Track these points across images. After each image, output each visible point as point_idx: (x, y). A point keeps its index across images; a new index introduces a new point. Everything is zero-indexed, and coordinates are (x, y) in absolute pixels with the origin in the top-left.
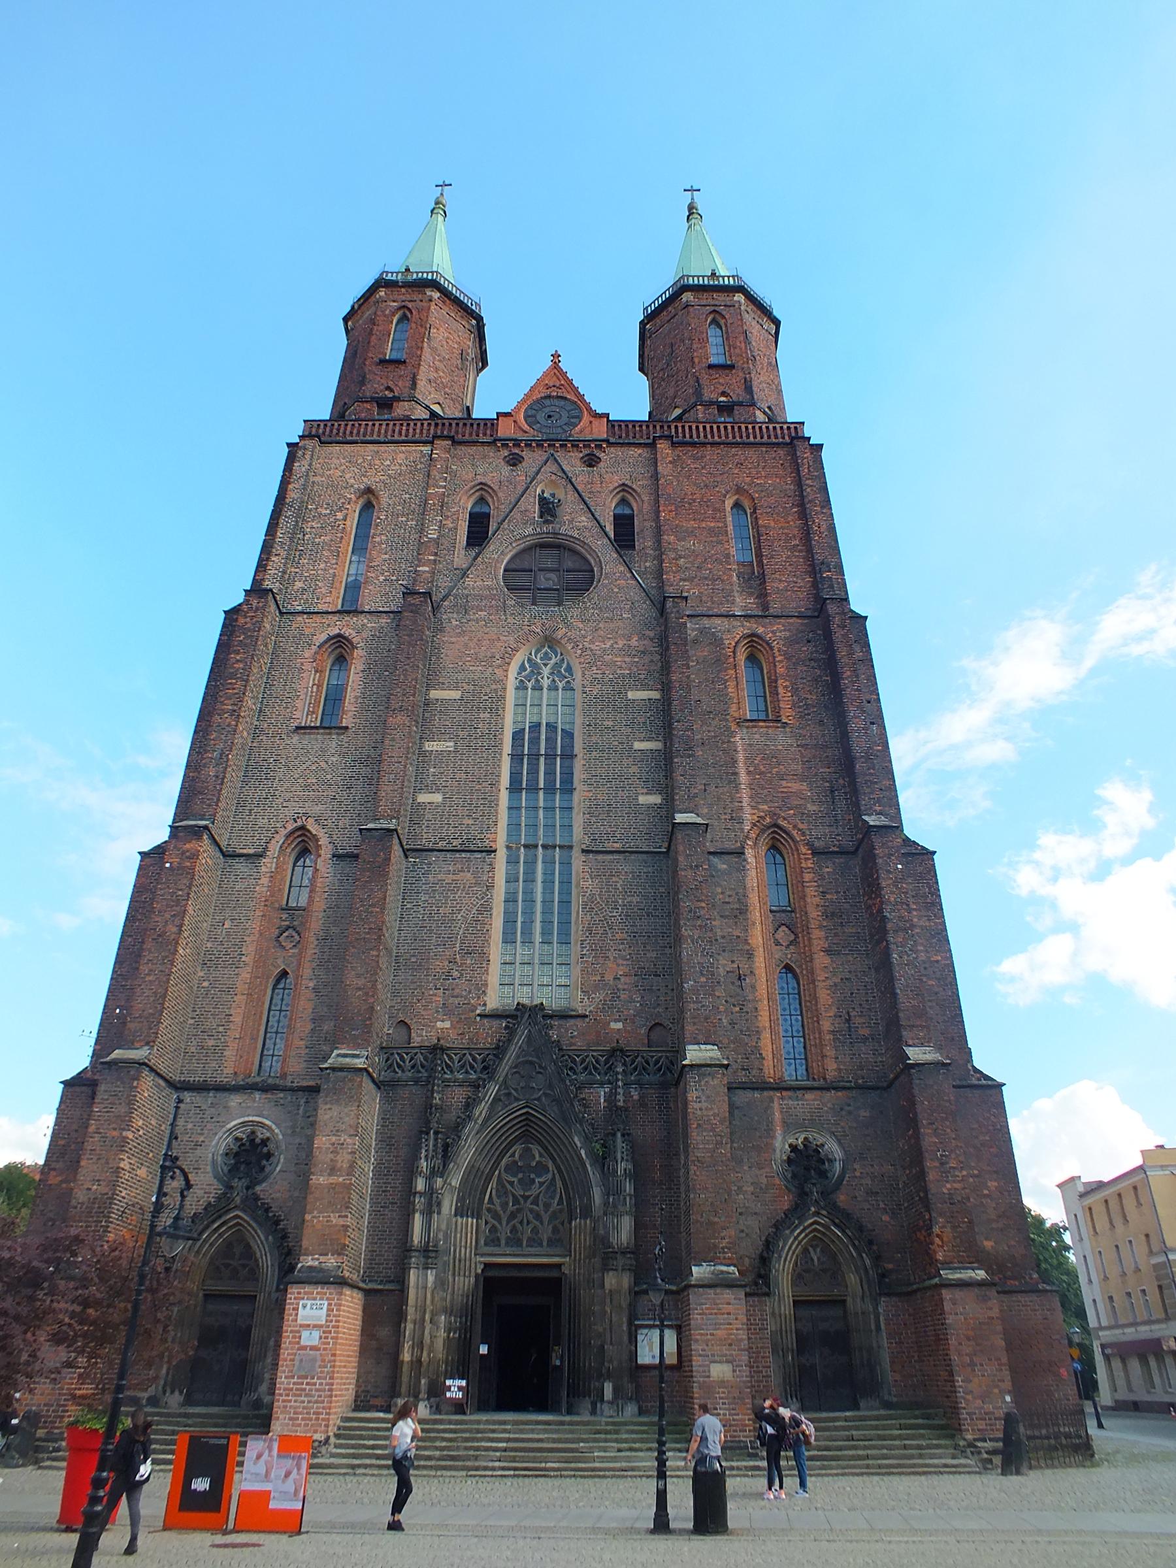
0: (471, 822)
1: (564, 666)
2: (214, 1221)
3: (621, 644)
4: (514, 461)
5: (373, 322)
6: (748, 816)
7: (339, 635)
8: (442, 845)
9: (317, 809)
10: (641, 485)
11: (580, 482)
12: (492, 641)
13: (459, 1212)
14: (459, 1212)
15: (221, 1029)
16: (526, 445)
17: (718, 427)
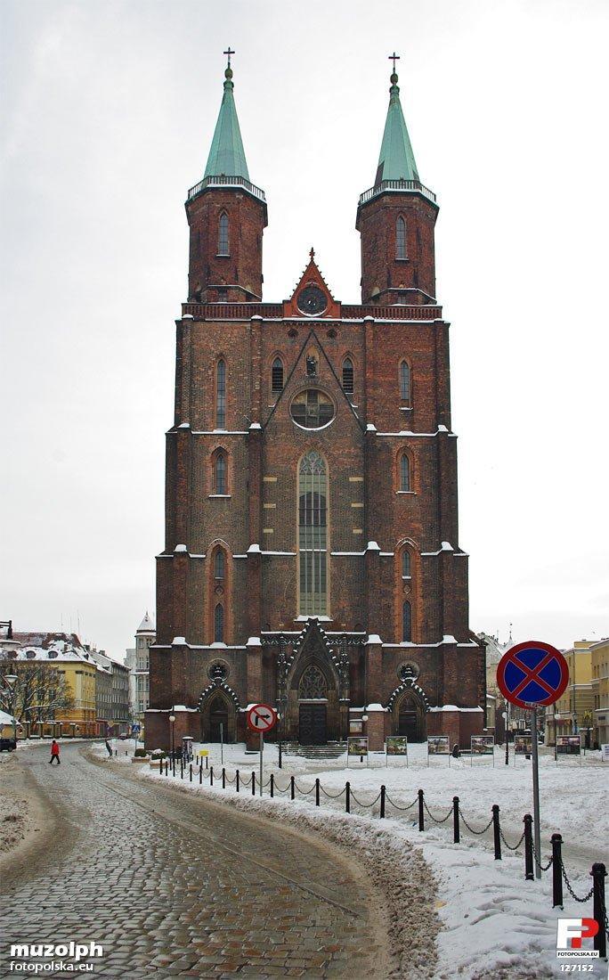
10: (357, 351)
13: (292, 688)
14: (292, 688)
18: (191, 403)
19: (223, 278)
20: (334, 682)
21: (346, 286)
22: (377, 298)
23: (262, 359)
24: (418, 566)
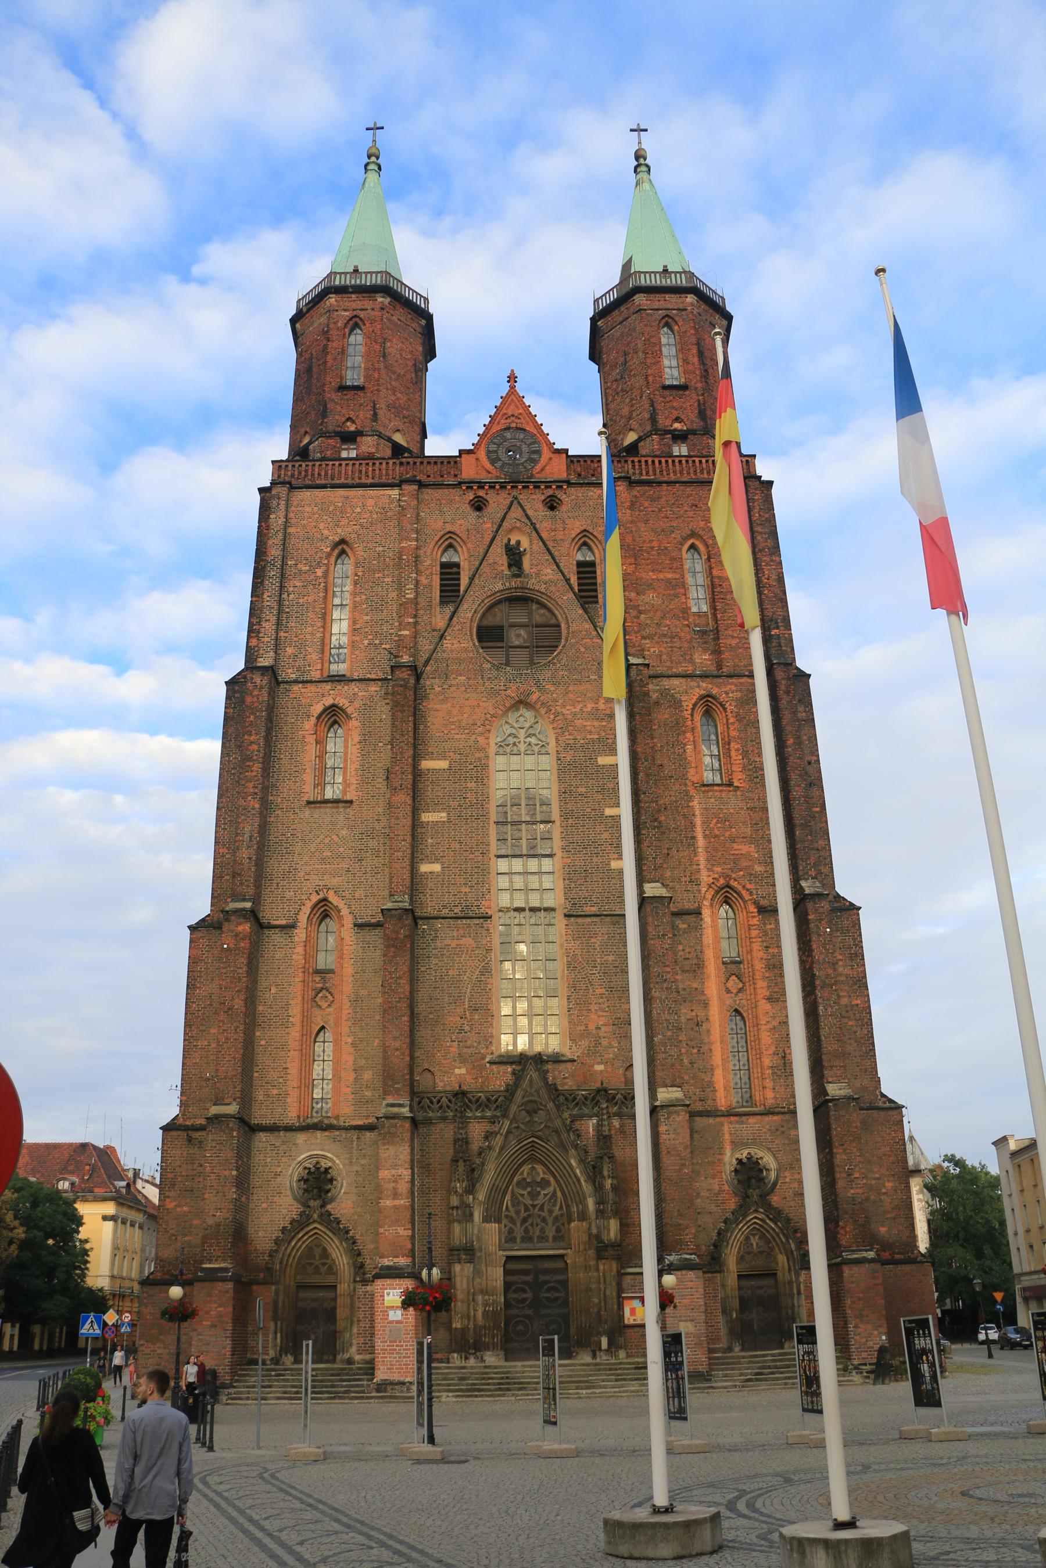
0: (468, 890)
2: (298, 1233)
3: (590, 706)
4: (479, 505)
5: (325, 333)
6: (705, 877)
7: (333, 705)
8: (445, 912)
9: (335, 881)
11: (543, 527)
12: (473, 707)
13: (486, 1219)
14: (486, 1219)
15: (281, 1080)
16: (490, 487)
17: (673, 461)
19: (349, 419)
20: (583, 1201)
22: (633, 449)
23: (417, 548)
24: (754, 933)
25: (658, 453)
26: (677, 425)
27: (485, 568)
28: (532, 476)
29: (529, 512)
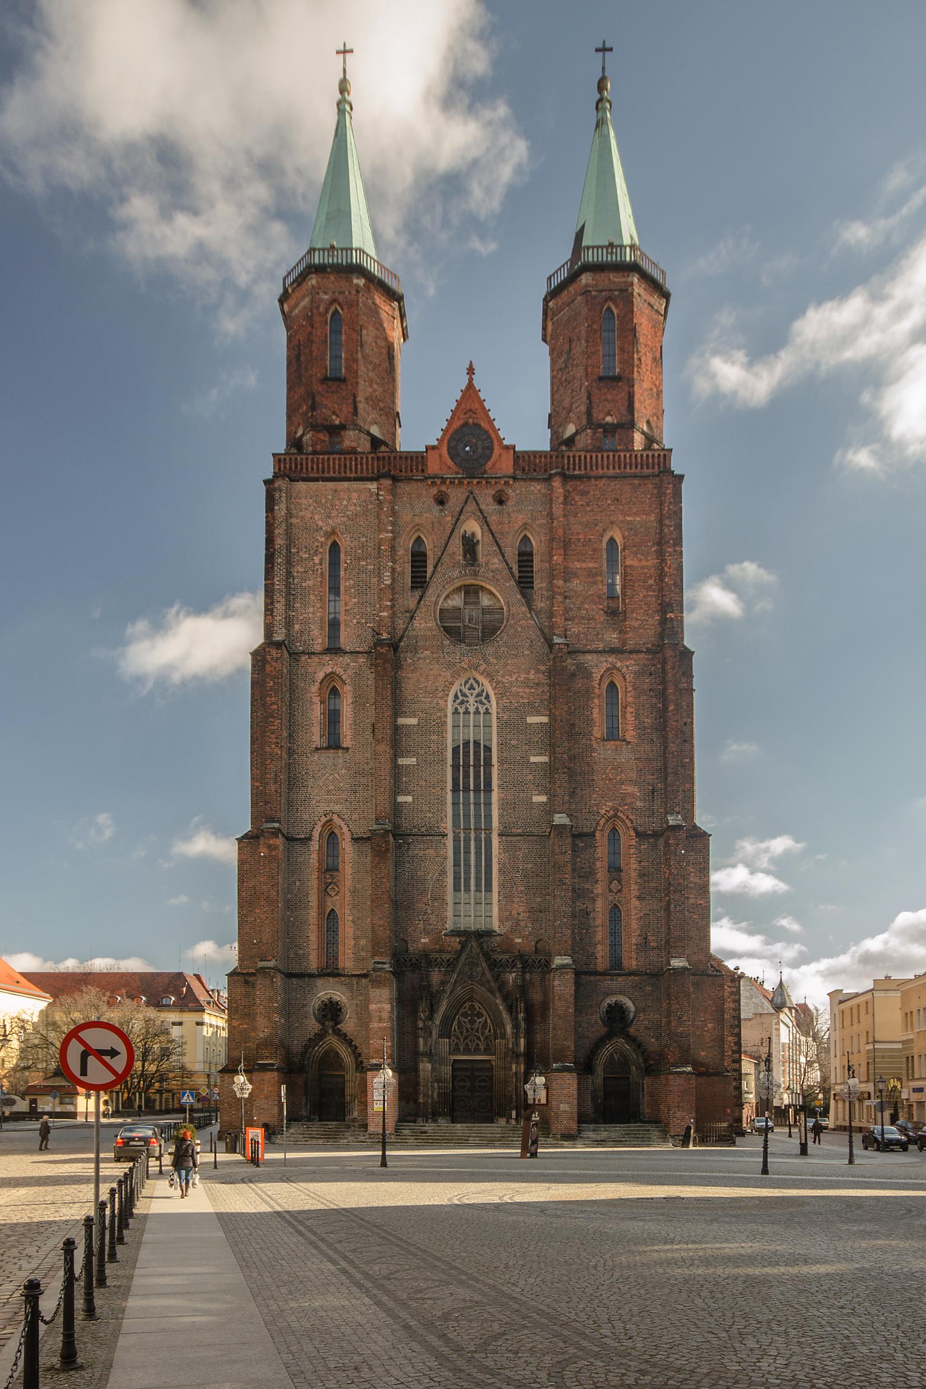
0: (431, 815)
1: (484, 694)
3: (523, 676)
7: (332, 673)
9: (337, 808)
11: (493, 519)
12: (436, 677)
13: (441, 1036)
18: (289, 606)
19: (334, 413)
21: (523, 420)
22: (570, 442)
23: (394, 539)
24: (632, 851)
25: (590, 448)
26: (609, 419)
27: (445, 558)
28: (485, 472)
29: (483, 507)
